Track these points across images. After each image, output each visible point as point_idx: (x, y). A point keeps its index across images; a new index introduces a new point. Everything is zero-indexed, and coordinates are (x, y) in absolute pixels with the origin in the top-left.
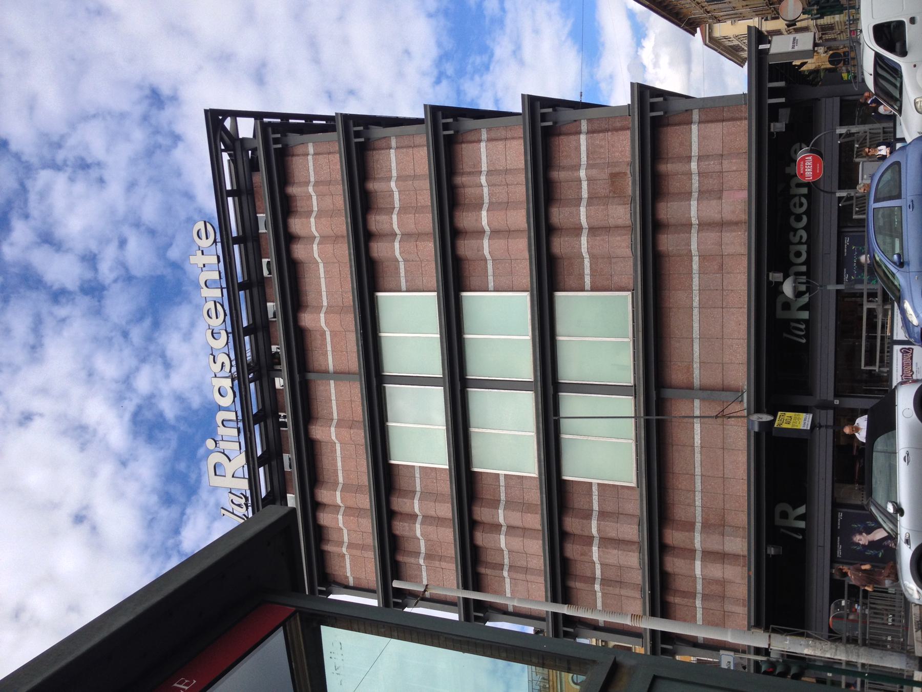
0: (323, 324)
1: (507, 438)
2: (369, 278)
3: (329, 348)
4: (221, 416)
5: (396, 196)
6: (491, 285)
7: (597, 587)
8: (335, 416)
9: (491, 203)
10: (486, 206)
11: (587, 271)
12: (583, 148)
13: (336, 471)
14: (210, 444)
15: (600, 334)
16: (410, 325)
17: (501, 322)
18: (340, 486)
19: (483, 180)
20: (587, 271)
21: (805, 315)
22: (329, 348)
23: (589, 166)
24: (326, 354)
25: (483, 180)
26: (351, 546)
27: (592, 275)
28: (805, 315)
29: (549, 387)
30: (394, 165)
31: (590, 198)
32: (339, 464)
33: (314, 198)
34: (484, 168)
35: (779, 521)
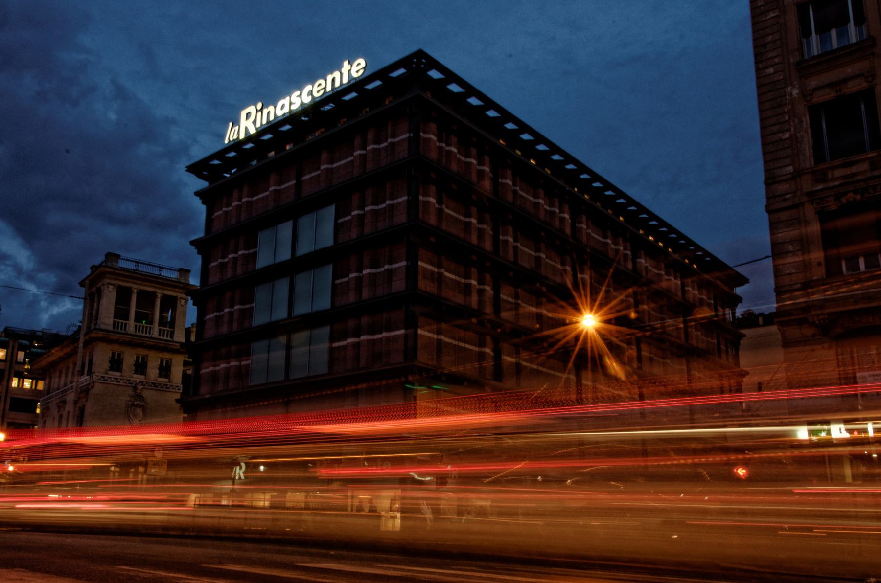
0: (322, 167)
1: (271, 305)
2: (339, 196)
3: (313, 174)
5: (383, 206)
6: (337, 282)
8: (282, 187)
9: (375, 274)
10: (374, 271)
13: (258, 194)
14: (259, 106)
16: (321, 230)
17: (317, 293)
18: (250, 199)
22: (313, 174)
23: (388, 339)
24: (310, 173)
26: (226, 212)
27: (339, 347)
30: (400, 200)
31: (374, 340)
32: (261, 196)
33: (385, 144)
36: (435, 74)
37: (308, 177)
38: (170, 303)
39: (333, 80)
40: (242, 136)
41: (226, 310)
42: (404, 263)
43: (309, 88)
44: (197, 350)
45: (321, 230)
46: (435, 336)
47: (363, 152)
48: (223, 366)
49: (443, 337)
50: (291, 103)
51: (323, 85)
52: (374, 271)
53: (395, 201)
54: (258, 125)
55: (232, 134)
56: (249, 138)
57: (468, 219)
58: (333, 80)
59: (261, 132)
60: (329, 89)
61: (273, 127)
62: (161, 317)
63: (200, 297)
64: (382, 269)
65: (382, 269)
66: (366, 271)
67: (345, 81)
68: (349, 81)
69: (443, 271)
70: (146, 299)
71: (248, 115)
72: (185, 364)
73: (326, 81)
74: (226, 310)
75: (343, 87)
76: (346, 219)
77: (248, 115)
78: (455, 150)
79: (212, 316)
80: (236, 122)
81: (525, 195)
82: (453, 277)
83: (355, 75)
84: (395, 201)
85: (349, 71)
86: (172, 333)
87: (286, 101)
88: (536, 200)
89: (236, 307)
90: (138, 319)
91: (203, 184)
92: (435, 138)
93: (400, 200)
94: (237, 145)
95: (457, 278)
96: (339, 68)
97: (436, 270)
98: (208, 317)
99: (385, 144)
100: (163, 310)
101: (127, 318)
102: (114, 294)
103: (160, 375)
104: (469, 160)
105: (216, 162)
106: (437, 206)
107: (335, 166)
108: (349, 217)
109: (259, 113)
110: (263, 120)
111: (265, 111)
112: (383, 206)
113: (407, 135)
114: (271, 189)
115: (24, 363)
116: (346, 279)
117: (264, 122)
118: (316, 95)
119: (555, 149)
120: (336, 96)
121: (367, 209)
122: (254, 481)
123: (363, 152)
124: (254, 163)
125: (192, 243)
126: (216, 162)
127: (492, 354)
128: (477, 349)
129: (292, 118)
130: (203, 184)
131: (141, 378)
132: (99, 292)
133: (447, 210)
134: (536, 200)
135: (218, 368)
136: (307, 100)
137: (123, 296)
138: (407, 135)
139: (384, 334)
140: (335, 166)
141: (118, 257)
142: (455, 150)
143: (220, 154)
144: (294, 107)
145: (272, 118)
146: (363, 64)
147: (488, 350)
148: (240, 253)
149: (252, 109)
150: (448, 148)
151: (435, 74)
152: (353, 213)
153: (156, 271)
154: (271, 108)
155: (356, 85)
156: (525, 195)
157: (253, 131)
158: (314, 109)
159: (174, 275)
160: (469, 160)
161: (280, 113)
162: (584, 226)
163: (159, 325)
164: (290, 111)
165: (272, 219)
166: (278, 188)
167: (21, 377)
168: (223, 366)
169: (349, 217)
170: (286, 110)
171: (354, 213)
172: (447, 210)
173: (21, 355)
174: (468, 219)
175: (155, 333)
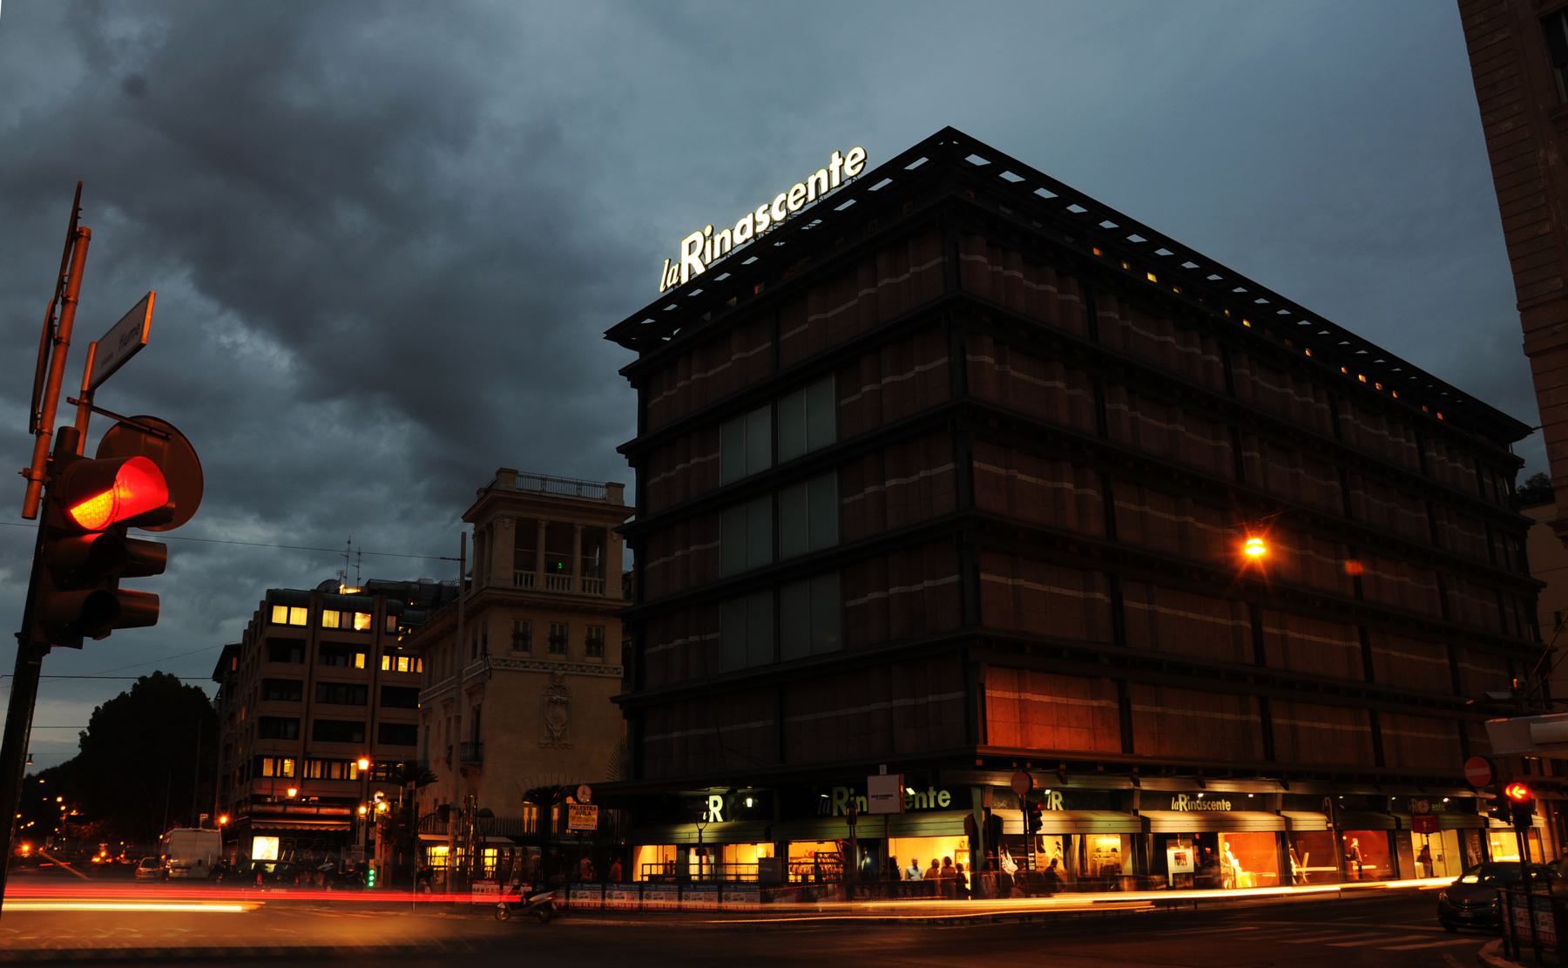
1: (746, 545)
2: (839, 363)
4: (726, 233)
5: (910, 375)
6: (846, 501)
7: (661, 647)
10: (903, 481)
11: (860, 601)
12: (949, 580)
14: (708, 231)
15: (816, 622)
16: (813, 423)
17: (814, 520)
19: (922, 474)
20: (860, 601)
21: (835, 814)
25: (922, 474)
28: (835, 814)
29: (778, 578)
30: (935, 364)
33: (907, 276)
34: (935, 471)
35: (712, 799)
36: (976, 160)
37: (788, 335)
38: (595, 539)
39: (817, 183)
40: (685, 279)
41: (678, 553)
42: (950, 466)
43: (782, 197)
44: (644, 617)
45: (813, 423)
46: (1010, 582)
47: (872, 291)
48: (678, 642)
49: (1022, 582)
50: (755, 224)
51: (803, 192)
52: (903, 481)
53: (929, 366)
54: (708, 260)
55: (667, 281)
56: (695, 281)
57: (1049, 384)
58: (817, 183)
59: (711, 272)
60: (811, 196)
61: (731, 262)
62: (585, 563)
63: (636, 538)
64: (915, 478)
65: (915, 478)
66: (890, 483)
67: (836, 182)
68: (842, 183)
69: (1014, 472)
70: (560, 538)
71: (692, 246)
72: (625, 631)
73: (806, 185)
74: (678, 553)
75: (833, 192)
76: (853, 398)
77: (692, 246)
78: (1020, 275)
79: (655, 563)
80: (675, 259)
81: (1143, 332)
82: (1034, 480)
83: (849, 172)
84: (929, 366)
85: (841, 167)
86: (602, 585)
87: (748, 221)
88: (1162, 339)
89: (692, 548)
90: (551, 568)
91: (632, 356)
92: (985, 260)
93: (935, 364)
94: (679, 292)
95: (1040, 481)
96: (826, 164)
97: (1002, 471)
98: (651, 565)
99: (907, 276)
100: (586, 550)
101: (532, 567)
102: (513, 532)
103: (589, 653)
104: (1043, 287)
105: (649, 321)
106: (997, 367)
107: (830, 314)
108: (858, 396)
109: (709, 243)
110: (714, 254)
111: (717, 239)
112: (910, 375)
113: (940, 259)
114: (734, 358)
115: (397, 633)
116: (859, 496)
117: (717, 254)
118: (793, 207)
119: (1183, 252)
120: (824, 207)
121: (884, 381)
122: (742, 829)
123: (872, 291)
124: (708, 316)
125: (620, 450)
126: (649, 321)
127: (1108, 600)
128: (1081, 595)
129: (760, 244)
130: (632, 356)
131: (561, 657)
132: (490, 526)
133: (1013, 373)
134: (1162, 339)
135: (671, 646)
136: (779, 216)
137: (525, 535)
138: (940, 259)
139: (926, 583)
140: (830, 314)
141: (515, 472)
142: (1020, 275)
143: (655, 309)
144: (760, 229)
145: (727, 248)
146: (861, 156)
147: (1099, 596)
148: (693, 461)
149: (697, 237)
150: (1007, 273)
151: (976, 160)
152: (864, 390)
153: (571, 491)
154: (726, 233)
155: (856, 188)
156: (1143, 332)
157: (700, 269)
158: (791, 227)
159: (600, 494)
160: (1043, 287)
161: (739, 239)
162: (1247, 372)
163: (583, 575)
164: (755, 235)
165: (739, 405)
166: (745, 355)
167: (394, 655)
168: (678, 642)
169: (858, 396)
170: (749, 234)
171: (866, 389)
172: (1013, 373)
173: (391, 622)
174: (1049, 384)
175: (576, 587)
